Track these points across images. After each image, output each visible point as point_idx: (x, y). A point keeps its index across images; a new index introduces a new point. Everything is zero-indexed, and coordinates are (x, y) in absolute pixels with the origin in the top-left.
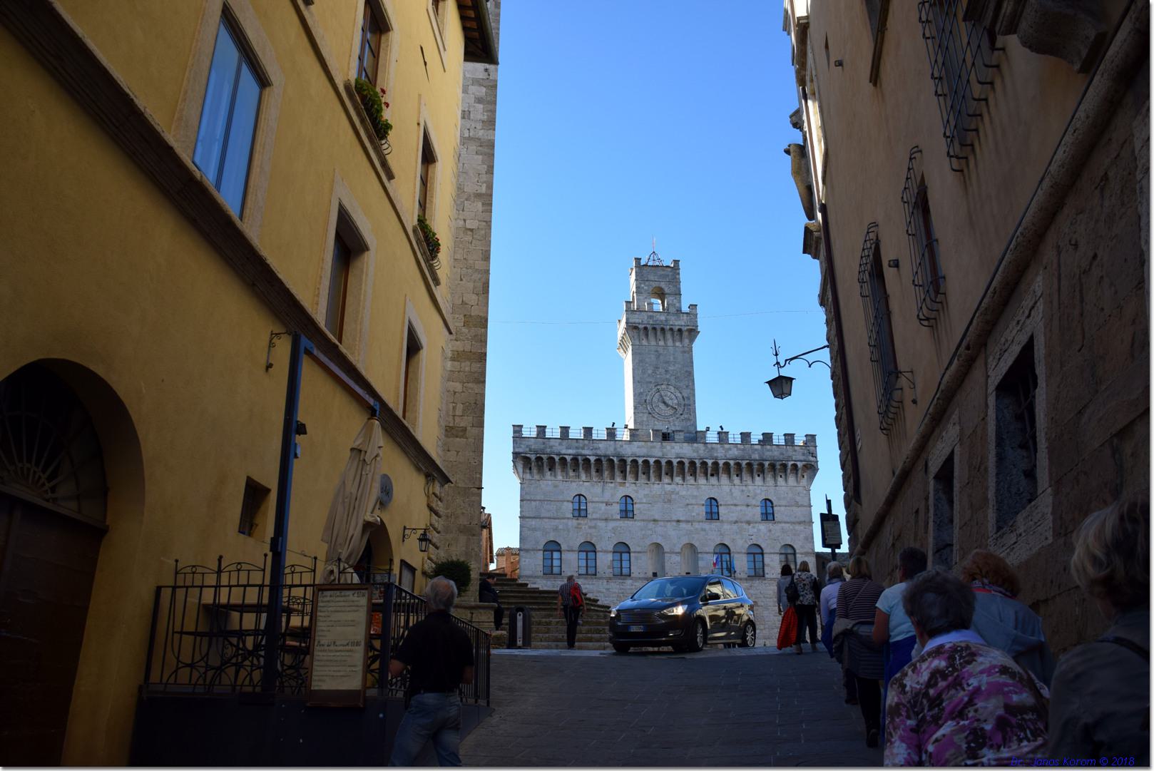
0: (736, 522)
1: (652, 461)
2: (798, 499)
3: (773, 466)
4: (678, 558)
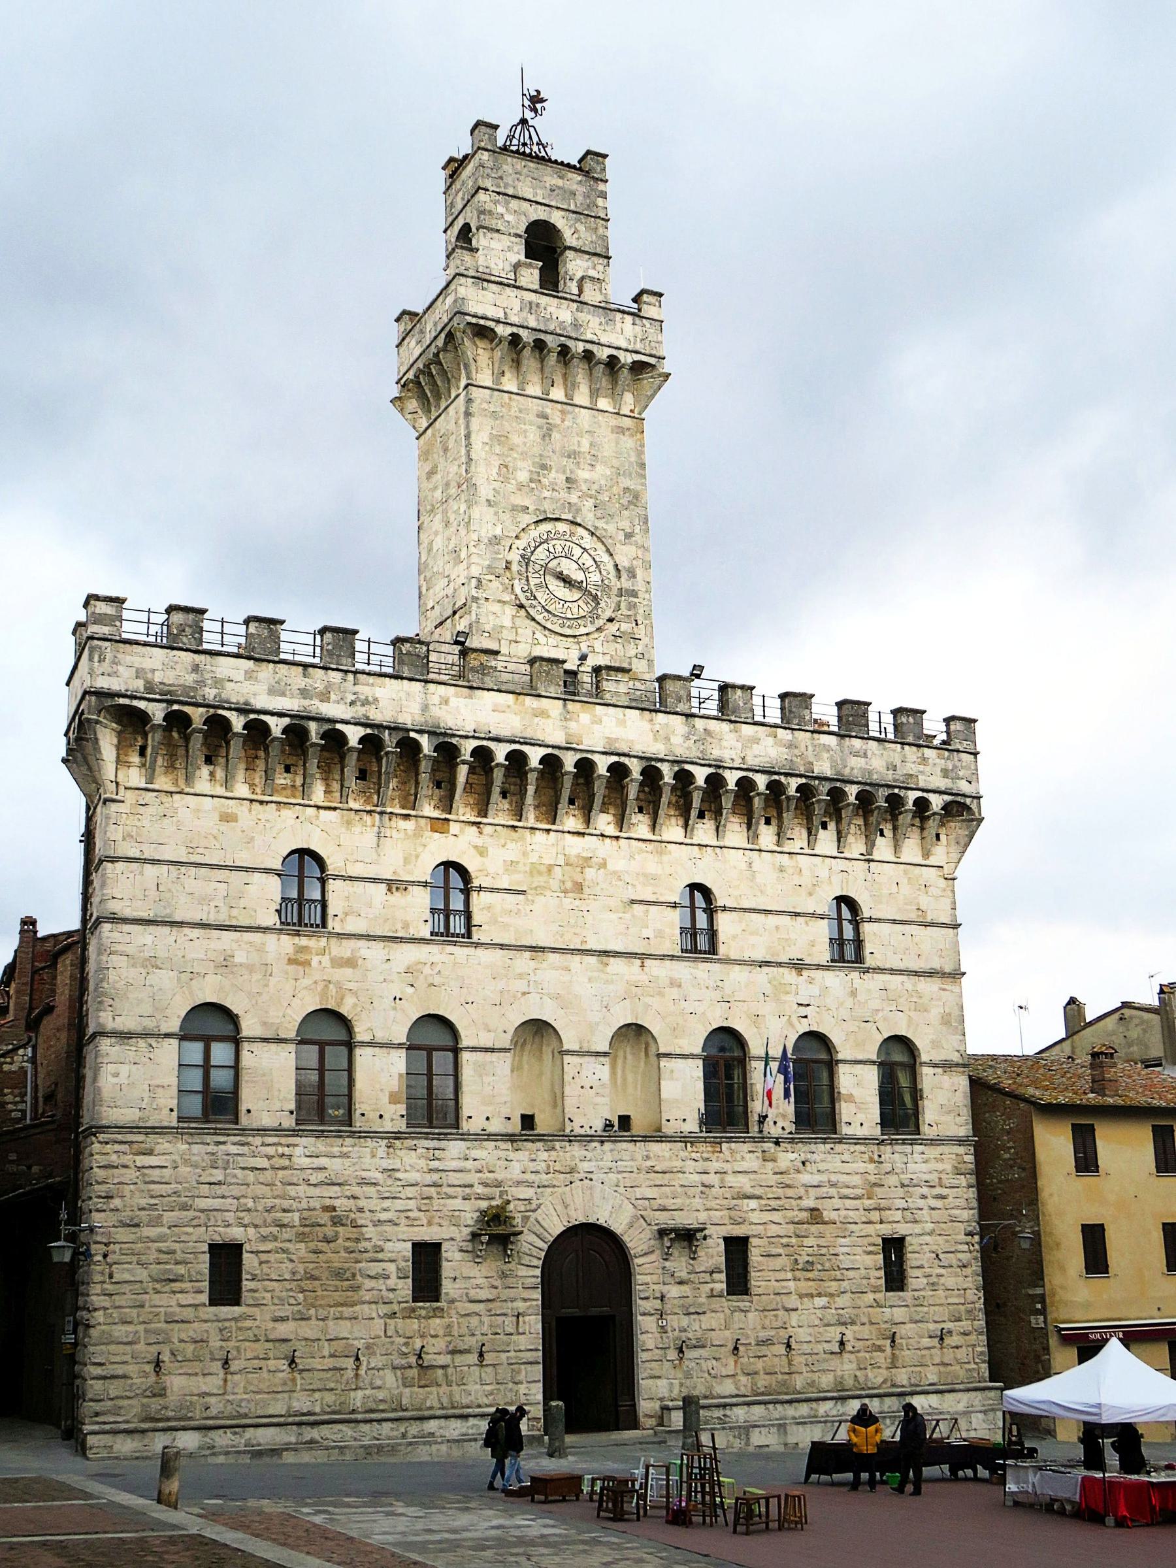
2: (924, 901)
3: (865, 800)
4: (600, 1071)
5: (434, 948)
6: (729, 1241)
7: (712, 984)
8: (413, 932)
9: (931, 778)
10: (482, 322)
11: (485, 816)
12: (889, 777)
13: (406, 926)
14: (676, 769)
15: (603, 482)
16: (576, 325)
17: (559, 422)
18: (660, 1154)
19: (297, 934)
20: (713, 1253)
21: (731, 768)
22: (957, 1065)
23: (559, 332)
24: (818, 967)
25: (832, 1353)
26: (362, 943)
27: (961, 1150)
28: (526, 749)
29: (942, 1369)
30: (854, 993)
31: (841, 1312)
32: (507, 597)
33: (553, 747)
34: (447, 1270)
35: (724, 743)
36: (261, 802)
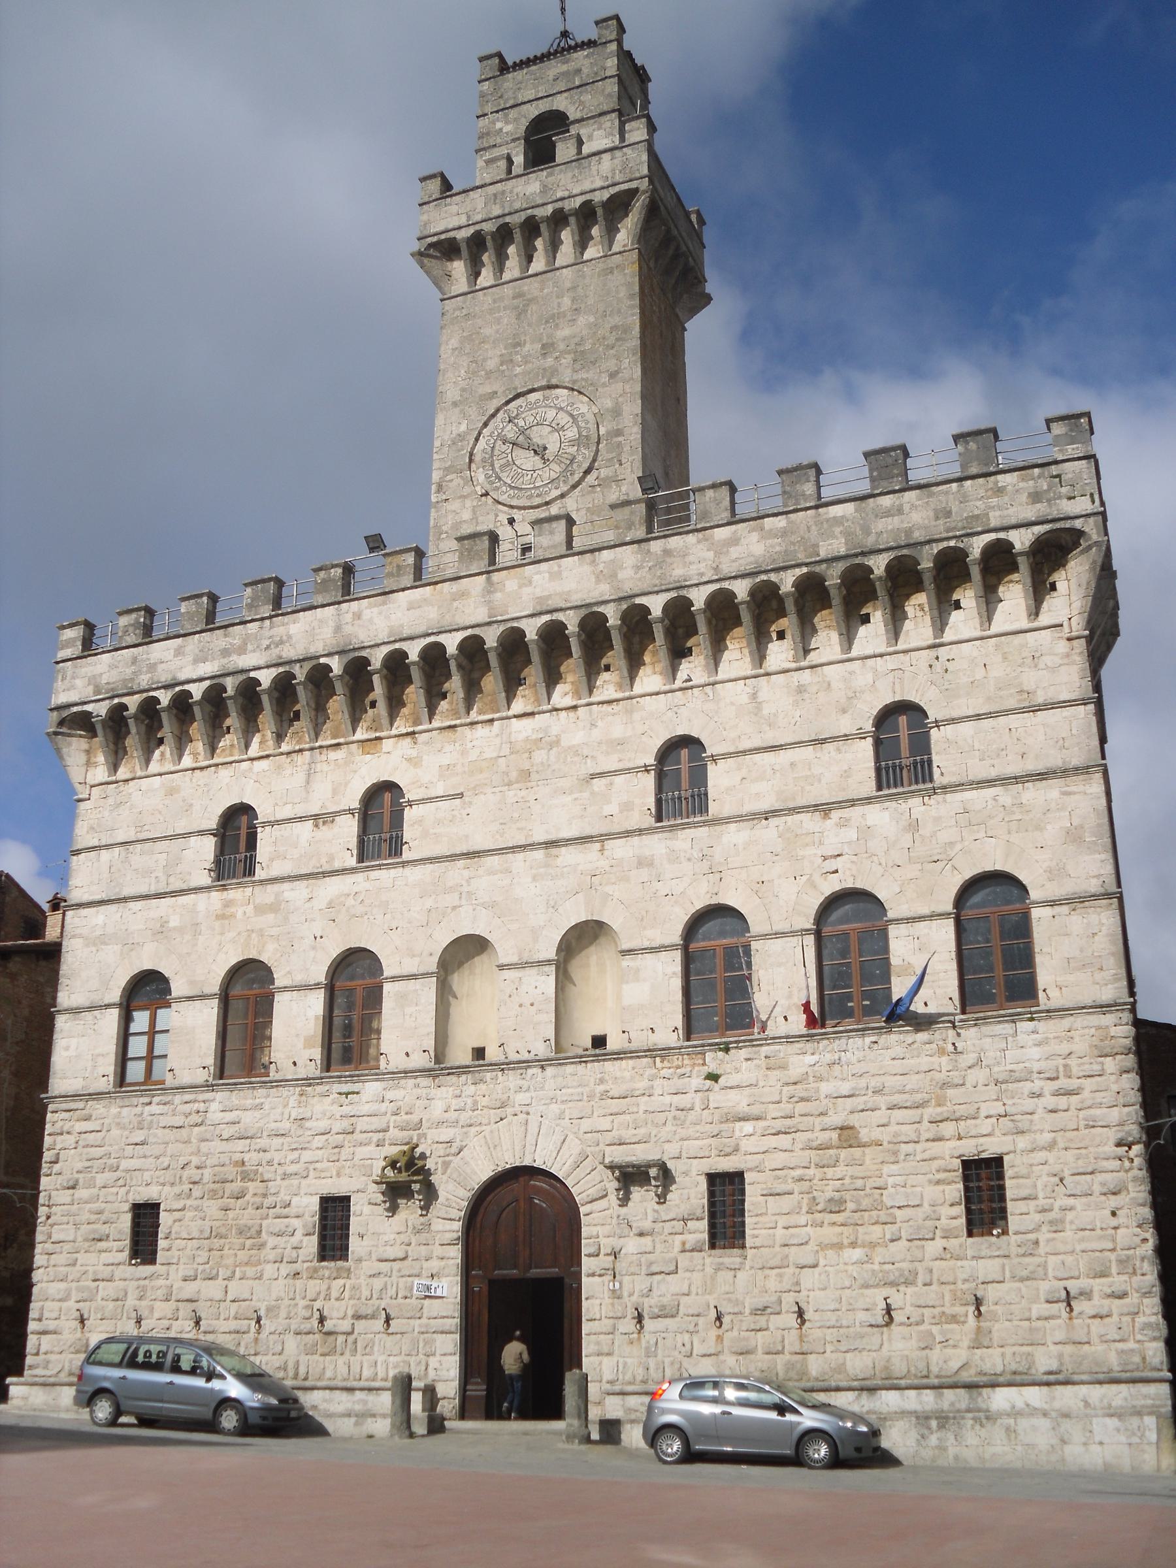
0: (767, 815)
1: (451, 643)
2: (1030, 678)
5: (359, 877)
6: (714, 1179)
7: (696, 854)
8: (337, 865)
9: (1011, 511)
10: (443, 237)
11: (417, 722)
12: (939, 528)
13: (331, 858)
14: (625, 606)
15: (584, 333)
16: (545, 189)
17: (536, 293)
18: (618, 1074)
19: (224, 888)
20: (691, 1193)
21: (697, 585)
22: (1095, 897)
23: (525, 206)
24: (853, 802)
25: (871, 1326)
26: (286, 886)
27: (1109, 1019)
28: (441, 639)
29: (1069, 1349)
30: (914, 826)
31: (887, 1267)
32: (467, 490)
33: (472, 627)
34: (355, 1225)
35: (691, 558)
36: (202, 769)
